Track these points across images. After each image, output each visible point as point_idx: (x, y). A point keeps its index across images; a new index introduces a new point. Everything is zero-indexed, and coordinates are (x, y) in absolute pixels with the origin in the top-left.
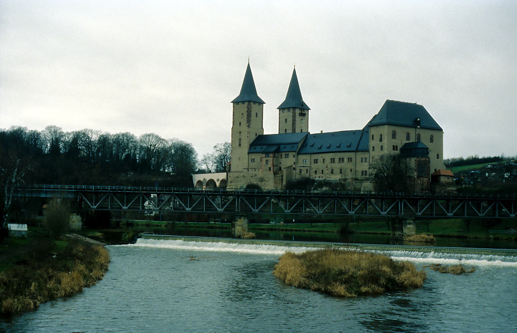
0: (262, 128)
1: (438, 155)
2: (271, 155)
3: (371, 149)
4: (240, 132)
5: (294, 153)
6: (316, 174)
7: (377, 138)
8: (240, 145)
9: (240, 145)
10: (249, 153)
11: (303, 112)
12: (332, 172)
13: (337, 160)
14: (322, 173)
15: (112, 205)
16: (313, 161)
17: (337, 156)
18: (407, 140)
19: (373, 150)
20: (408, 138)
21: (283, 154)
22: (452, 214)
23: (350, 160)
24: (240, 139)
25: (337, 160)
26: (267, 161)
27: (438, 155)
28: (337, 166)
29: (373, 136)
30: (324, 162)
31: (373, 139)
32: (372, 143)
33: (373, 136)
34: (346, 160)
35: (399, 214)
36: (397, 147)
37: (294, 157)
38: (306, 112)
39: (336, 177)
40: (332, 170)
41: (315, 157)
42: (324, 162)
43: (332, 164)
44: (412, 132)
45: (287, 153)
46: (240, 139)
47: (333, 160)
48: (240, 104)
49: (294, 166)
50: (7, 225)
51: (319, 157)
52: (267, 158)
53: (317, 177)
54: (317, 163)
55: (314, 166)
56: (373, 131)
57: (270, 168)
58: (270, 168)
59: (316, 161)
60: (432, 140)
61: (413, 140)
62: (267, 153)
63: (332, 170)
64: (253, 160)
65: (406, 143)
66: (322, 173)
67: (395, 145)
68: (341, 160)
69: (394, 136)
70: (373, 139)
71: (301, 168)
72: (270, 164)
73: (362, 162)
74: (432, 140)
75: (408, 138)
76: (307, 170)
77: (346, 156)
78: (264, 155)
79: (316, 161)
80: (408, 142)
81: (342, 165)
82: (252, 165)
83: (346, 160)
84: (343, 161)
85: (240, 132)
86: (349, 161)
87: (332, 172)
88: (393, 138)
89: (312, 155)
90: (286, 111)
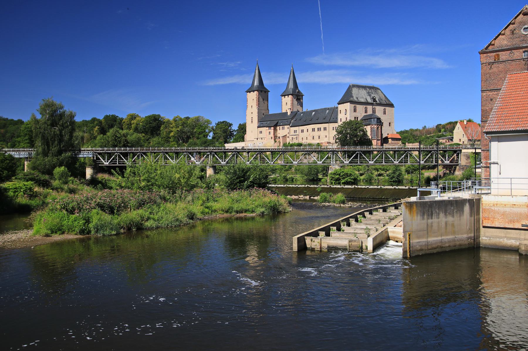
0: (268, 109)
1: (390, 123)
2: (272, 128)
3: (339, 120)
4: (252, 113)
5: (288, 126)
6: (303, 140)
7: (343, 112)
8: (252, 122)
9: (252, 122)
10: (258, 127)
11: (299, 98)
12: (313, 138)
13: (316, 130)
14: (307, 139)
15: (120, 161)
16: (300, 131)
17: (316, 126)
18: (365, 113)
19: (341, 121)
20: (366, 112)
21: (281, 127)
22: (373, 162)
23: (325, 129)
24: (252, 118)
25: (316, 130)
26: (270, 132)
27: (390, 123)
28: (316, 133)
29: (340, 111)
30: (308, 131)
31: (340, 113)
32: (340, 116)
33: (340, 111)
34: (322, 129)
35: (332, 163)
36: (357, 118)
37: (288, 129)
38: (300, 97)
39: (316, 141)
40: (313, 137)
41: (301, 128)
42: (308, 131)
43: (313, 132)
44: (370, 108)
45: (283, 126)
46: (252, 118)
47: (313, 130)
48: (252, 93)
49: (288, 135)
50: (87, 180)
51: (305, 128)
52: (270, 130)
53: (304, 142)
54: (303, 132)
55: (301, 135)
56: (341, 107)
57: (272, 137)
58: (272, 137)
59: (302, 131)
60: (385, 113)
61: (370, 112)
62: (270, 127)
63: (313, 137)
64: (261, 132)
65: (365, 116)
66: (307, 139)
67: (356, 117)
68: (319, 129)
69: (355, 110)
70: (340, 113)
71: (293, 136)
72: (272, 135)
73: (333, 129)
74: (385, 113)
75: (366, 112)
76: (297, 137)
77: (322, 126)
78: (268, 128)
79: (302, 131)
80: (366, 114)
81: (319, 133)
82: (261, 136)
83: (322, 129)
84: (320, 130)
85: (252, 113)
86: (324, 130)
87: (313, 138)
88: (354, 112)
89: (300, 127)
90: (286, 97)
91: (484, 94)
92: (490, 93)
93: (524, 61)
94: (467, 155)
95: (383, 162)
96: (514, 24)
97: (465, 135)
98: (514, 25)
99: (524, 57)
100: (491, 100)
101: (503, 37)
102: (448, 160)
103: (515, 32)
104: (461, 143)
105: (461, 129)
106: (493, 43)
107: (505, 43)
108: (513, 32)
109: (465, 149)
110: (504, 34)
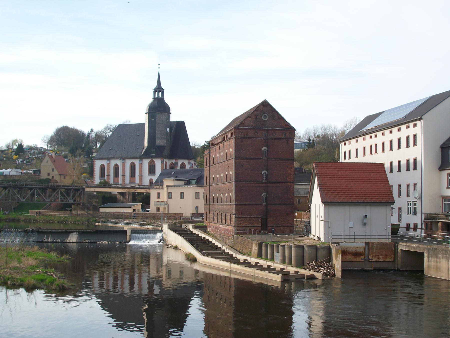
91: (237, 161)
92: (241, 161)
93: (264, 139)
94: (90, 194)
95: (9, 200)
96: (257, 111)
97: (55, 170)
98: (257, 112)
99: (264, 137)
100: (242, 166)
101: (250, 119)
102: (72, 199)
103: (258, 117)
104: (50, 177)
105: (50, 163)
106: (243, 122)
107: (251, 124)
108: (256, 117)
109: (88, 187)
110: (250, 117)
